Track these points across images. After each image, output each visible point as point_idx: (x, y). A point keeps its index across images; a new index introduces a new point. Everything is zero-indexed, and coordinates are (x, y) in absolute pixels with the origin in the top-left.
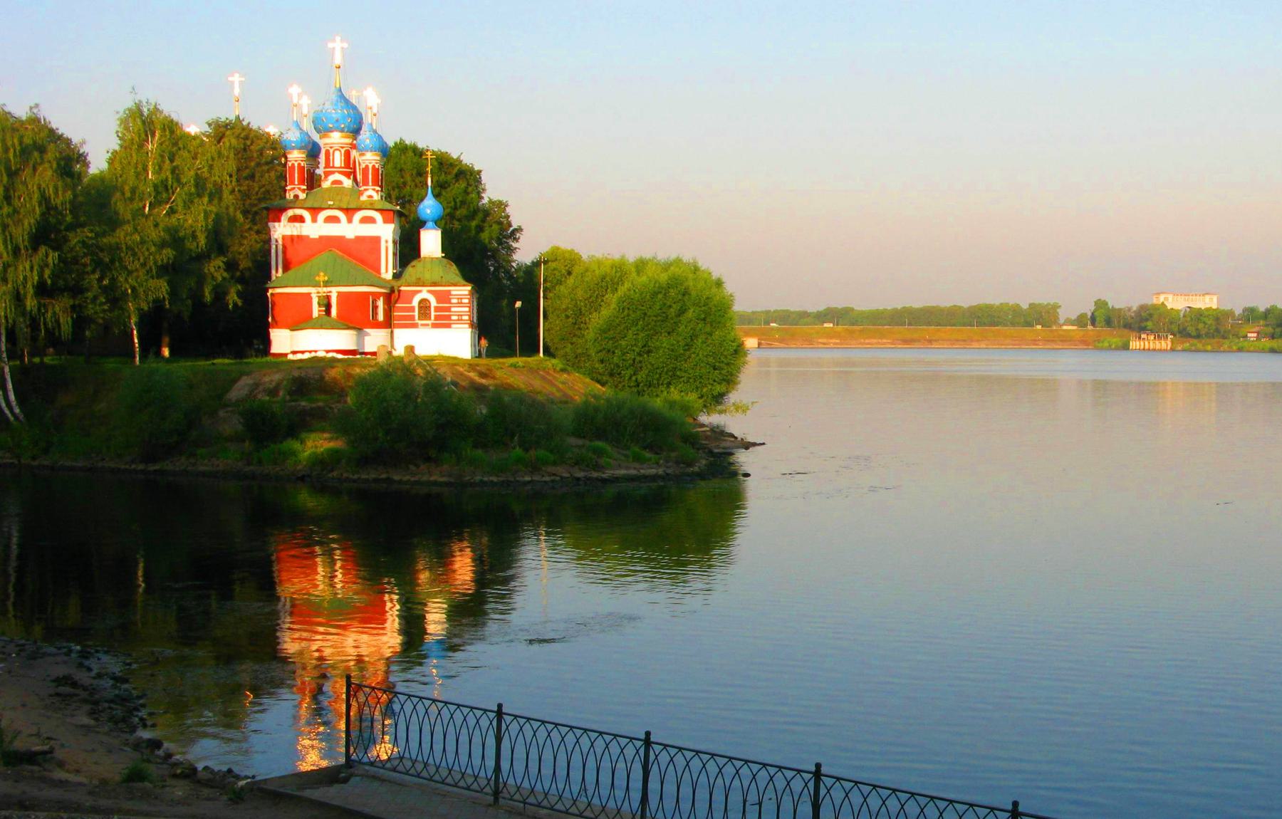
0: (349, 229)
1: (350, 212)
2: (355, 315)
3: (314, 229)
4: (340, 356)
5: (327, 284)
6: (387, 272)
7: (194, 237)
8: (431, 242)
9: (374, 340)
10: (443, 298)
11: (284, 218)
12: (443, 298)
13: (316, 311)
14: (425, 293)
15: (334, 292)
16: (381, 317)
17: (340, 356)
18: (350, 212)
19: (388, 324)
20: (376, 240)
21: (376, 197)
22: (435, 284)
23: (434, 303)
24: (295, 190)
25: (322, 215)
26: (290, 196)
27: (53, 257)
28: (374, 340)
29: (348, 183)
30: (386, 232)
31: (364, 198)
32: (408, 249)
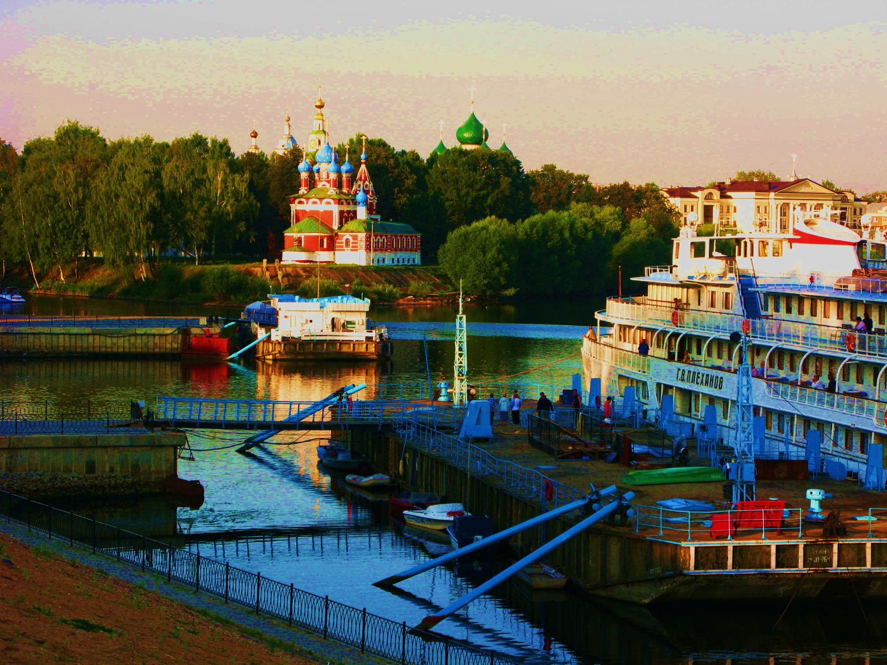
0: (321, 207)
1: (321, 199)
2: (313, 245)
3: (308, 207)
4: (297, 263)
5: (299, 232)
6: (335, 226)
7: (228, 214)
8: (362, 213)
9: (322, 256)
10: (355, 238)
11: (297, 201)
12: (355, 238)
13: (296, 243)
14: (348, 236)
15: (302, 235)
16: (325, 246)
17: (297, 263)
18: (321, 199)
19: (331, 247)
20: (331, 213)
21: (334, 193)
22: (352, 232)
23: (351, 240)
24: (303, 190)
25: (311, 201)
26: (301, 192)
27: (152, 225)
28: (322, 256)
29: (328, 185)
30: (335, 209)
31: (329, 193)
32: (347, 217)
